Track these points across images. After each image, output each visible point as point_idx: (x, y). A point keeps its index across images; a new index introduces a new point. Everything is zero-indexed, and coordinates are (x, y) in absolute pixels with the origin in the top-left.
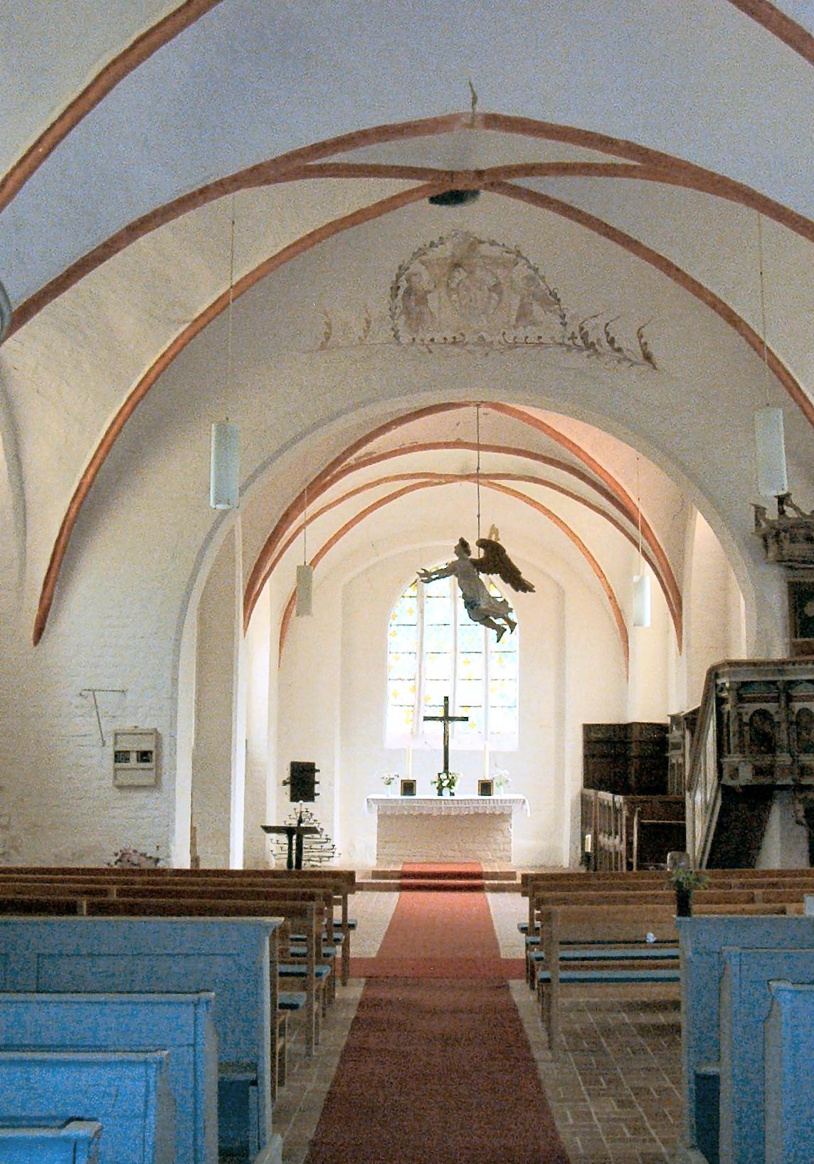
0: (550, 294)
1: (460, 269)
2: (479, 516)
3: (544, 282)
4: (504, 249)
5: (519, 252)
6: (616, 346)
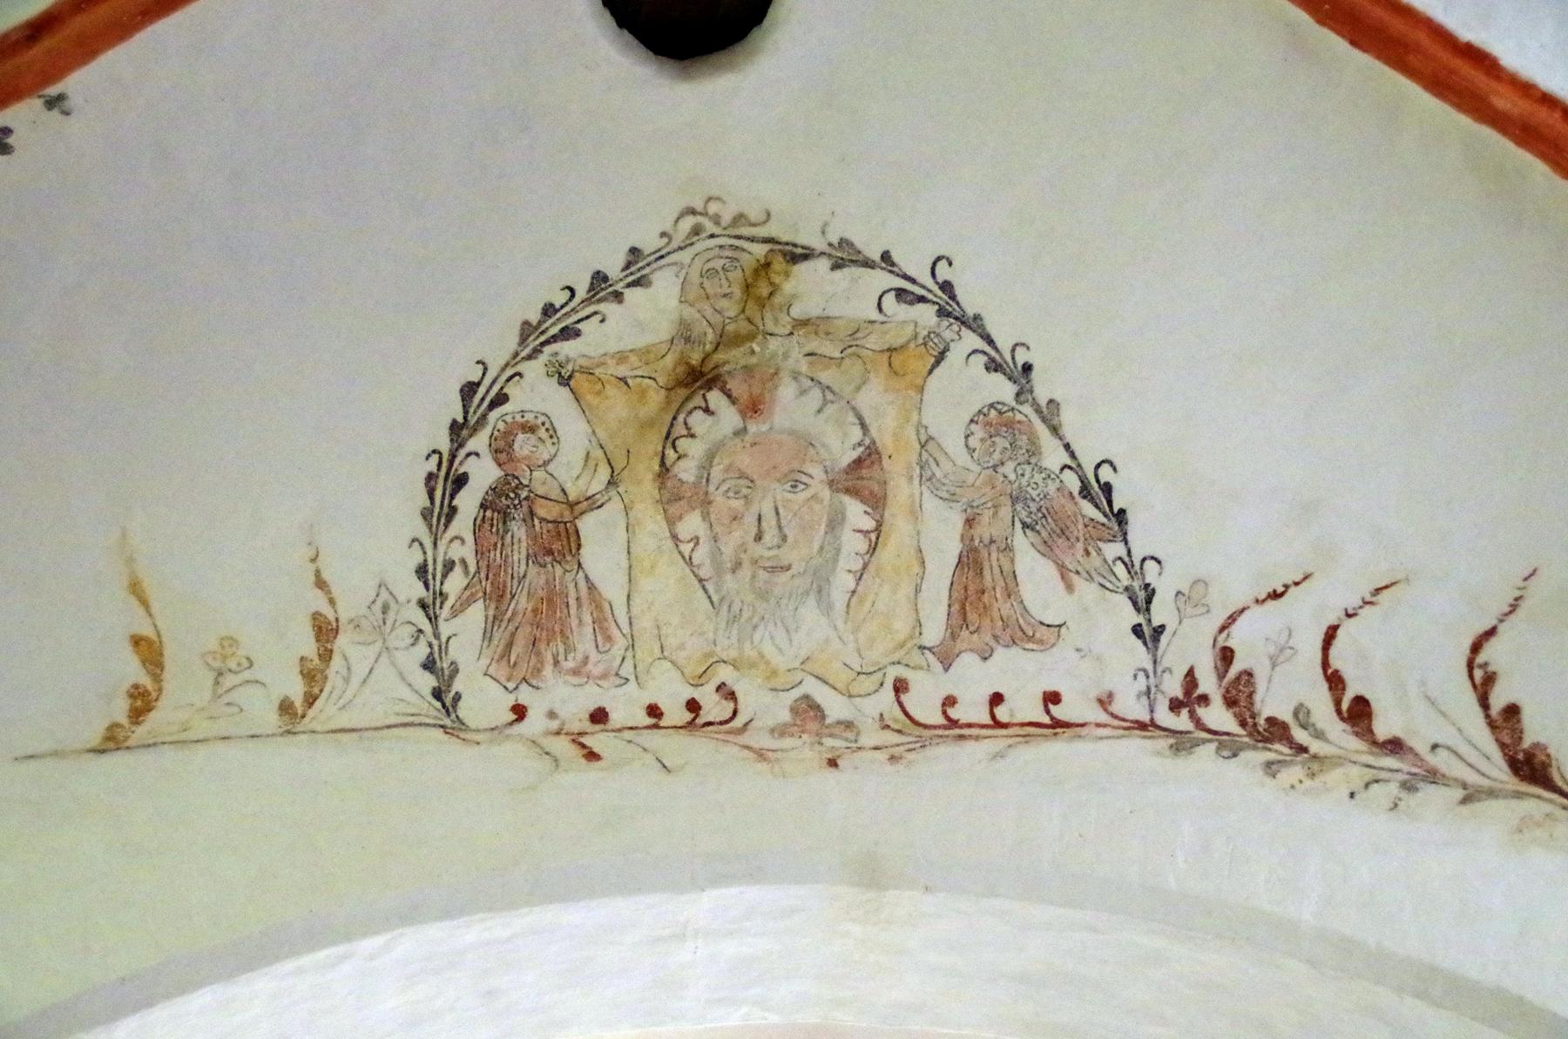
0: (1085, 491)
1: (715, 398)
3: (1055, 430)
4: (883, 280)
5: (947, 287)
6: (1383, 730)
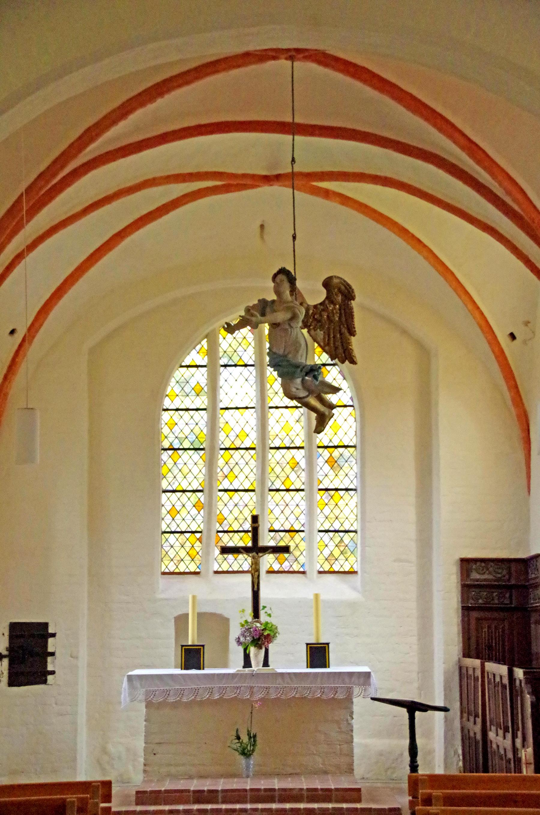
2: (294, 238)
